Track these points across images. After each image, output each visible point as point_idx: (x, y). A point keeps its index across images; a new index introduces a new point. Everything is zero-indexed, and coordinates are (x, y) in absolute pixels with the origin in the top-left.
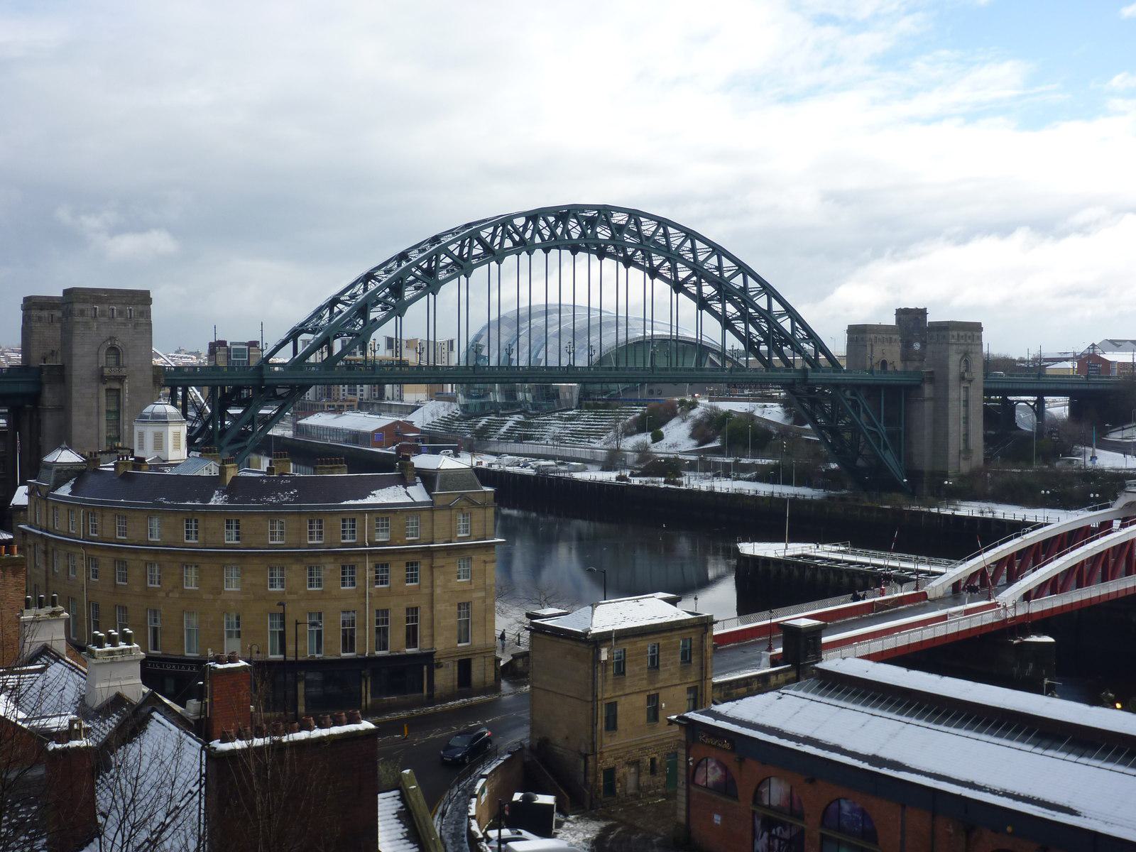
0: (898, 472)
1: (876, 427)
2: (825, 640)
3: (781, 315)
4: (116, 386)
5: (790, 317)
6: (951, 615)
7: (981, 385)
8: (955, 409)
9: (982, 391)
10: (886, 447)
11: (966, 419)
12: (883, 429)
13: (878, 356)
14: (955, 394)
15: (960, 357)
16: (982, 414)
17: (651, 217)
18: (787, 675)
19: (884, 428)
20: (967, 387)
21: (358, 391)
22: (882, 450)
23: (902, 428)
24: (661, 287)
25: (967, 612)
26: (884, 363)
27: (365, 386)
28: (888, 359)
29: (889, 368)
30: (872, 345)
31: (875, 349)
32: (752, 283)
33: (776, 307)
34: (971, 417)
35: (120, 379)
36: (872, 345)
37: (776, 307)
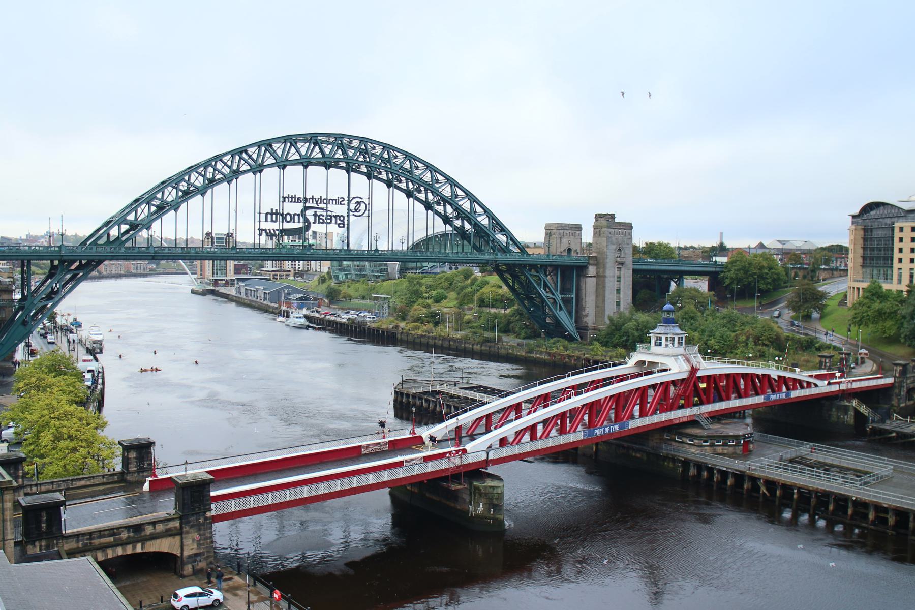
1: (553, 295)
2: (213, 494)
3: (480, 215)
5: (487, 216)
6: (406, 461)
7: (631, 267)
8: (611, 284)
9: (631, 271)
10: (561, 309)
11: (618, 291)
12: (559, 297)
13: (565, 245)
14: (611, 272)
16: (631, 287)
17: (380, 144)
18: (167, 525)
19: (560, 296)
20: (620, 268)
21: (297, 265)
22: (558, 311)
23: (574, 296)
24: (400, 197)
25: (427, 459)
26: (569, 250)
27: (301, 262)
28: (573, 247)
29: (573, 254)
32: (460, 193)
33: (479, 209)
37: (479, 209)
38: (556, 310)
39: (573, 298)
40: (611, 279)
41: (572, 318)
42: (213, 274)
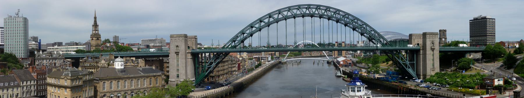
0: (414, 74)
1: (406, 62)
4: (178, 54)
9: (439, 52)
10: (409, 68)
11: (433, 60)
12: (408, 63)
15: (430, 42)
16: (439, 58)
19: (408, 62)
22: (408, 69)
23: (415, 62)
30: (414, 39)
31: (415, 40)
34: (435, 59)
35: (179, 52)
36: (414, 39)
38: (407, 68)
39: (414, 63)
40: (429, 55)
41: (414, 71)
42: (338, 55)
